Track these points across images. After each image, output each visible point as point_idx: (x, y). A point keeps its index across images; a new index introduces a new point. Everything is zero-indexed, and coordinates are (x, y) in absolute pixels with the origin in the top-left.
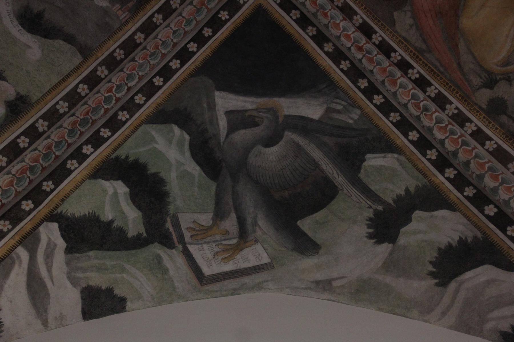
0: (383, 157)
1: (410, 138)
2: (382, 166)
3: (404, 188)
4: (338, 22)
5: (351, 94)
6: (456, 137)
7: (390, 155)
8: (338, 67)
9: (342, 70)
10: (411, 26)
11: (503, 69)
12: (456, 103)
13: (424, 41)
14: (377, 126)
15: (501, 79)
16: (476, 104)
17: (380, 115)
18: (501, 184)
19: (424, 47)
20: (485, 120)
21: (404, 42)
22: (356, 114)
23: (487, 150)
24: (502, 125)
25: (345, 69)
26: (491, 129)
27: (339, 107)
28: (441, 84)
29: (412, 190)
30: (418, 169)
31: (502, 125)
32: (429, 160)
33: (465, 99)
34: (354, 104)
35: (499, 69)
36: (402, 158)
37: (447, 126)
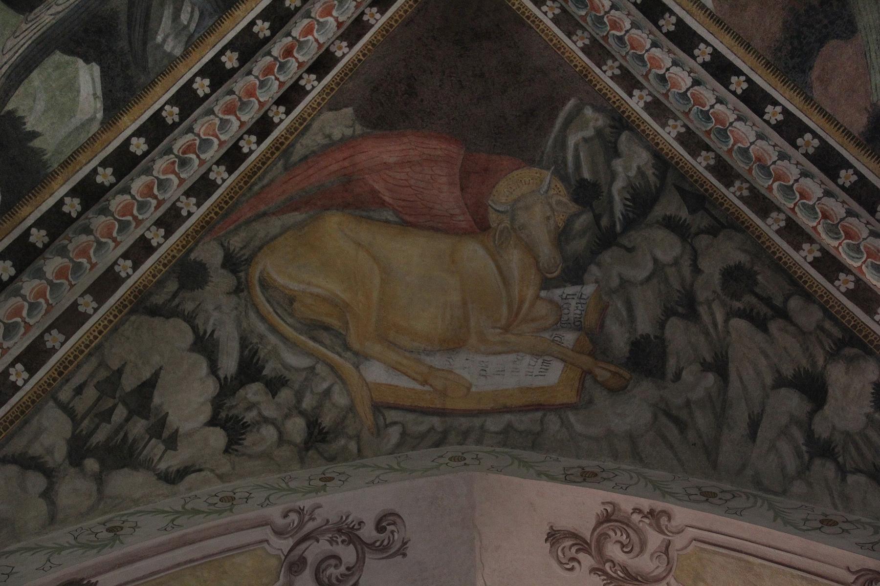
0: (95, 94)
1: (134, 140)
2: (79, 91)
3: (39, 129)
4: (334, 13)
5: (212, 39)
6: (135, 212)
7: (99, 105)
8: (258, 17)
9: (253, 23)
10: (329, 136)
11: (256, 282)
12: (199, 213)
13: (305, 158)
14: (153, 83)
15: (238, 279)
16: (196, 244)
17: (174, 90)
18: (50, 283)
19: (295, 158)
20: (169, 258)
21: (303, 127)
22: (174, 47)
23: (115, 263)
24: (161, 284)
25: (255, 29)
26: (153, 267)
27: (184, 18)
28: (231, 188)
29: (36, 143)
30: (76, 153)
31: (161, 284)
32: (94, 171)
33: (206, 227)
34: (192, 44)
35: (255, 274)
36: (95, 127)
37: (156, 197)
